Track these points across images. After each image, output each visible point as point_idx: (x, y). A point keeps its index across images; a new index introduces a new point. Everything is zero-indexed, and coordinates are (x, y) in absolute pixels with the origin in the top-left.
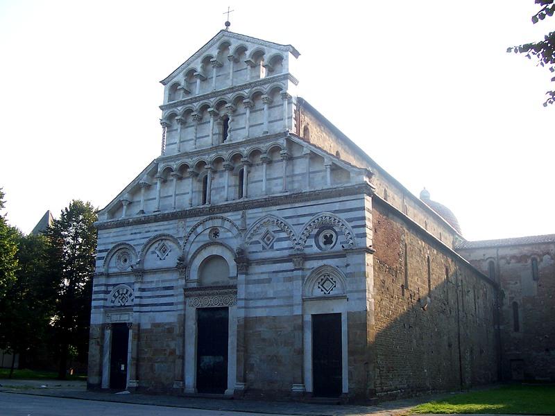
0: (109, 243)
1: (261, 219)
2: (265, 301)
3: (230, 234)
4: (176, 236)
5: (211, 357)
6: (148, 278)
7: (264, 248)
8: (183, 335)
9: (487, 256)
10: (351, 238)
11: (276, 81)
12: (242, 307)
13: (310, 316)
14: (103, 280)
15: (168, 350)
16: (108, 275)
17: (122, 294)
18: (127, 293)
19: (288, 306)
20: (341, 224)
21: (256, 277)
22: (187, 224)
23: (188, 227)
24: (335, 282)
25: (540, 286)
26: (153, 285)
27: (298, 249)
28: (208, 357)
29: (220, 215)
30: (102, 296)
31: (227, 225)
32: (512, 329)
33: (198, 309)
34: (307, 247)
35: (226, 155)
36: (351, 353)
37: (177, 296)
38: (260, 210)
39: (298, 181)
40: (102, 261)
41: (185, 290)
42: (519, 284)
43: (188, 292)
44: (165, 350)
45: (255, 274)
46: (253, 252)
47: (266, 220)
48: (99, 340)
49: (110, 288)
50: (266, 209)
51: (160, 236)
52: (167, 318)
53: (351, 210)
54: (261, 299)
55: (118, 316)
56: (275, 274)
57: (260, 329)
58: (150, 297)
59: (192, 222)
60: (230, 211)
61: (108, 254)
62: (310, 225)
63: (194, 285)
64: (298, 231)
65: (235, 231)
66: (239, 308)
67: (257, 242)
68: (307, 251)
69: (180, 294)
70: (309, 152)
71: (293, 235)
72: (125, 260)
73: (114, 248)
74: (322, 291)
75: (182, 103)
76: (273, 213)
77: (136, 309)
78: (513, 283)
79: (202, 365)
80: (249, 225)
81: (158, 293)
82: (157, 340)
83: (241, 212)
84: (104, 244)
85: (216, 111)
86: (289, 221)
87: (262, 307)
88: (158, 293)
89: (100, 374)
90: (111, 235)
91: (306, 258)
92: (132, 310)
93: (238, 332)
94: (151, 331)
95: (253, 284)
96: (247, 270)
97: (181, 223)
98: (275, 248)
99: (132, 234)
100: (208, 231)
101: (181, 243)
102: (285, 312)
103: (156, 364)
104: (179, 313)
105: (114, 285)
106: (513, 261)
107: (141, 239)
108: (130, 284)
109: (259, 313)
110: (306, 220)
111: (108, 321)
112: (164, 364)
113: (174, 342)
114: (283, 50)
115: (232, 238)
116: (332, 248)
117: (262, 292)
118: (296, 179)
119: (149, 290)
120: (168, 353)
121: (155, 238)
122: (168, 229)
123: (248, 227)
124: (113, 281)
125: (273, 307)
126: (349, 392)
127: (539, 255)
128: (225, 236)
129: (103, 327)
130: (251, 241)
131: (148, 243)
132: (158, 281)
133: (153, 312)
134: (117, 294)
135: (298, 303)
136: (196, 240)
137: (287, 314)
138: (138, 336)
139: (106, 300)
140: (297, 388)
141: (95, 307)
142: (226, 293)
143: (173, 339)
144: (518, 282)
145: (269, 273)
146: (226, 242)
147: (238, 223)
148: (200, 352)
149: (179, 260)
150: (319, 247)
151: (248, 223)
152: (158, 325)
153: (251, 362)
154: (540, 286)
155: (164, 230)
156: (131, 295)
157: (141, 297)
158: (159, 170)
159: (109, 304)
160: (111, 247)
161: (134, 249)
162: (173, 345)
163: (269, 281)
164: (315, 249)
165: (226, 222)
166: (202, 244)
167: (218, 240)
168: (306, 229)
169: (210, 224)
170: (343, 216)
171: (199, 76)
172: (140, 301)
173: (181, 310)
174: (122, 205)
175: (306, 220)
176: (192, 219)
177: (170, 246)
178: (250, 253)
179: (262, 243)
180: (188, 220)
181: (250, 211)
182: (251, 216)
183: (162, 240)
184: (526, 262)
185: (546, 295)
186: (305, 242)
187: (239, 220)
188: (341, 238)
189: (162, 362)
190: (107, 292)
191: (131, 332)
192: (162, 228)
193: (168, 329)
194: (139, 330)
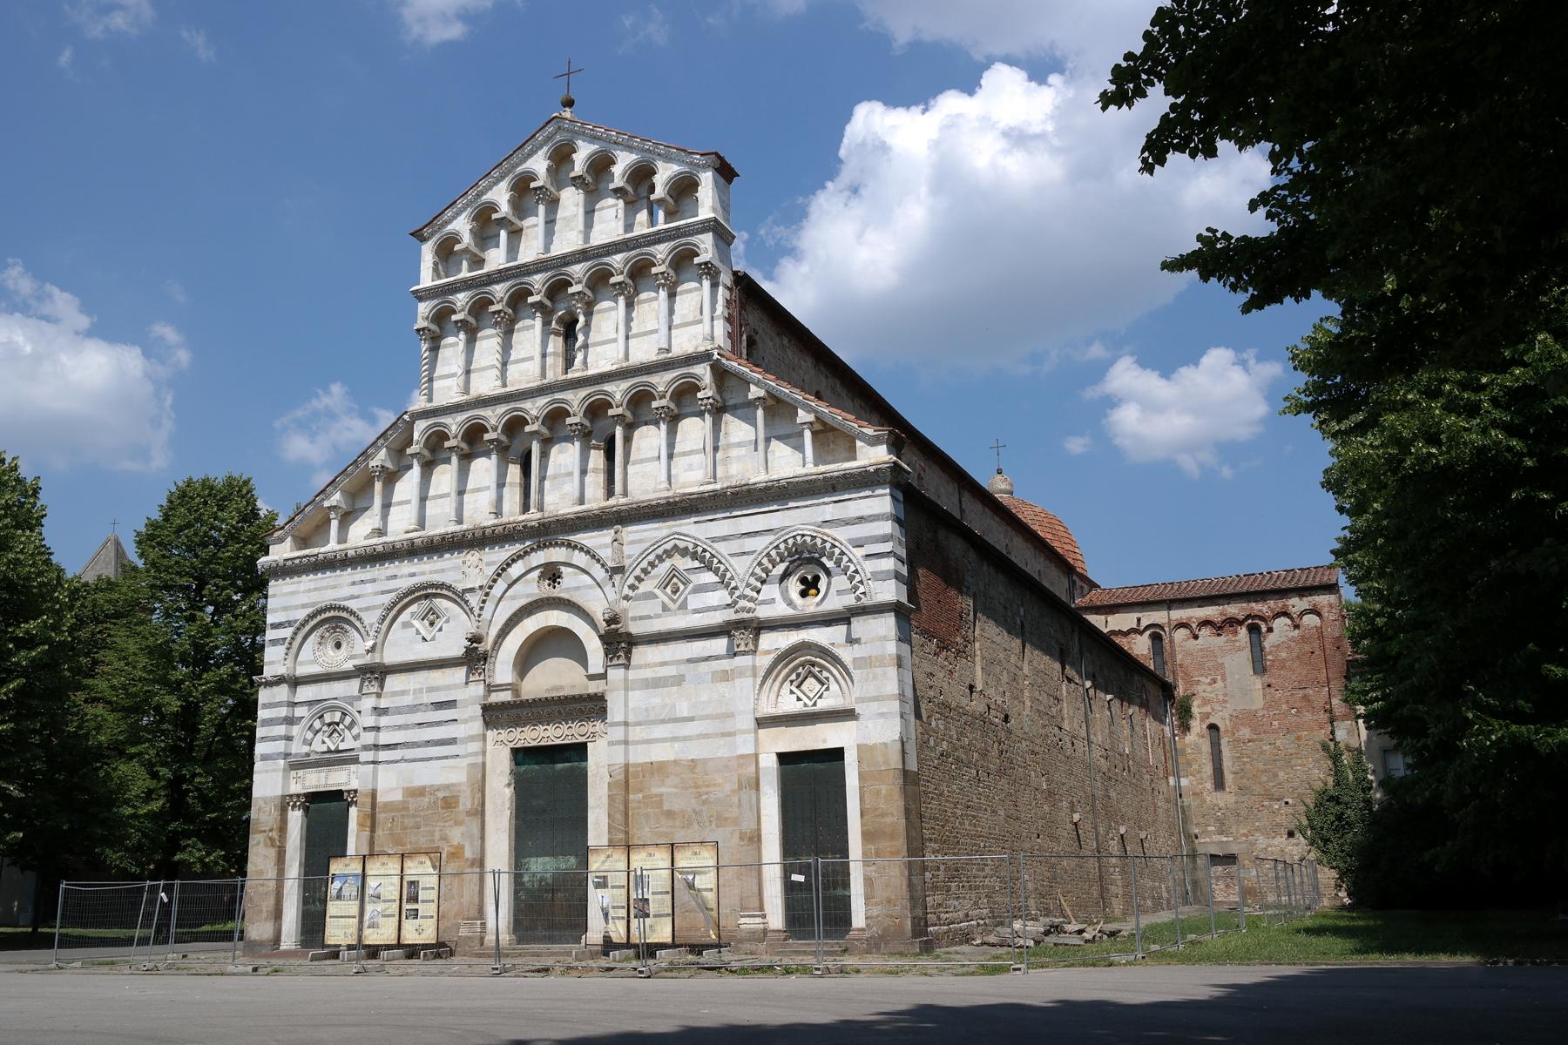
0: (296, 607)
1: (657, 543)
4: (460, 587)
5: (547, 859)
6: (393, 682)
7: (665, 608)
8: (480, 812)
9: (1144, 623)
10: (861, 582)
11: (685, 235)
12: (619, 743)
13: (775, 758)
14: (282, 692)
16: (295, 682)
17: (329, 725)
18: (342, 720)
19: (724, 735)
20: (837, 551)
21: (648, 674)
23: (488, 564)
24: (827, 678)
25: (1269, 686)
26: (408, 700)
27: (743, 609)
28: (540, 860)
30: (281, 730)
31: (579, 558)
32: (1209, 785)
34: (763, 603)
35: (575, 400)
36: (867, 836)
37: (465, 721)
39: (739, 458)
40: (281, 649)
41: (487, 709)
42: (1220, 684)
43: (494, 715)
45: (647, 666)
46: (641, 618)
48: (275, 834)
49: (300, 712)
52: (448, 773)
53: (861, 519)
54: (663, 721)
55: (323, 774)
57: (663, 790)
58: (400, 727)
59: (500, 554)
61: (295, 634)
62: (768, 555)
63: (505, 696)
64: (740, 568)
65: (599, 573)
66: (611, 743)
67: (650, 596)
68: (763, 613)
69: (472, 719)
70: (762, 393)
71: (732, 578)
72: (338, 645)
73: (311, 617)
74: (799, 699)
75: (466, 285)
77: (365, 756)
78: (1208, 680)
79: (526, 879)
80: (629, 557)
81: (419, 717)
84: (285, 609)
85: (548, 303)
86: (722, 548)
87: (664, 740)
88: (419, 717)
89: (278, 914)
90: (302, 587)
91: (759, 627)
92: (355, 761)
93: (611, 798)
94: (401, 807)
95: (641, 689)
96: (629, 659)
97: (473, 557)
99: (354, 583)
100: (536, 573)
101: (474, 600)
102: (719, 750)
104: (472, 760)
105: (310, 703)
106: (1205, 632)
107: (376, 594)
108: (351, 700)
109: (660, 753)
110: (760, 543)
111: (296, 788)
113: (462, 829)
114: (698, 165)
115: (590, 587)
116: (818, 605)
118: (734, 453)
119: (399, 711)
121: (410, 592)
122: (443, 571)
123: (627, 562)
124: (305, 692)
126: (868, 925)
127: (1263, 619)
129: (285, 803)
131: (395, 604)
132: (419, 691)
133: (406, 761)
134: (317, 724)
135: (745, 727)
137: (723, 753)
138: (371, 821)
139: (289, 738)
140: (749, 923)
141: (265, 758)
143: (458, 823)
144: (1219, 678)
145: (678, 662)
146: (577, 598)
147: (606, 554)
148: (521, 851)
149: (470, 640)
150: (790, 603)
151: (627, 550)
152: (420, 792)
154: (1269, 686)
155: (431, 572)
156: (353, 723)
157: (377, 729)
158: (416, 436)
159: (297, 748)
160: (301, 615)
161: (359, 619)
162: (456, 835)
163: (679, 680)
164: (780, 610)
165: (577, 552)
167: (558, 592)
168: (760, 564)
169: (540, 558)
170: (842, 534)
171: (503, 222)
172: (376, 738)
173: (475, 754)
174: (329, 521)
175: (760, 543)
177: (446, 609)
178: (634, 619)
181: (630, 528)
183: (427, 596)
184: (1235, 633)
185: (1284, 706)
186: (758, 592)
187: (606, 546)
188: (840, 582)
190: (290, 721)
191: (353, 811)
194: (374, 805)
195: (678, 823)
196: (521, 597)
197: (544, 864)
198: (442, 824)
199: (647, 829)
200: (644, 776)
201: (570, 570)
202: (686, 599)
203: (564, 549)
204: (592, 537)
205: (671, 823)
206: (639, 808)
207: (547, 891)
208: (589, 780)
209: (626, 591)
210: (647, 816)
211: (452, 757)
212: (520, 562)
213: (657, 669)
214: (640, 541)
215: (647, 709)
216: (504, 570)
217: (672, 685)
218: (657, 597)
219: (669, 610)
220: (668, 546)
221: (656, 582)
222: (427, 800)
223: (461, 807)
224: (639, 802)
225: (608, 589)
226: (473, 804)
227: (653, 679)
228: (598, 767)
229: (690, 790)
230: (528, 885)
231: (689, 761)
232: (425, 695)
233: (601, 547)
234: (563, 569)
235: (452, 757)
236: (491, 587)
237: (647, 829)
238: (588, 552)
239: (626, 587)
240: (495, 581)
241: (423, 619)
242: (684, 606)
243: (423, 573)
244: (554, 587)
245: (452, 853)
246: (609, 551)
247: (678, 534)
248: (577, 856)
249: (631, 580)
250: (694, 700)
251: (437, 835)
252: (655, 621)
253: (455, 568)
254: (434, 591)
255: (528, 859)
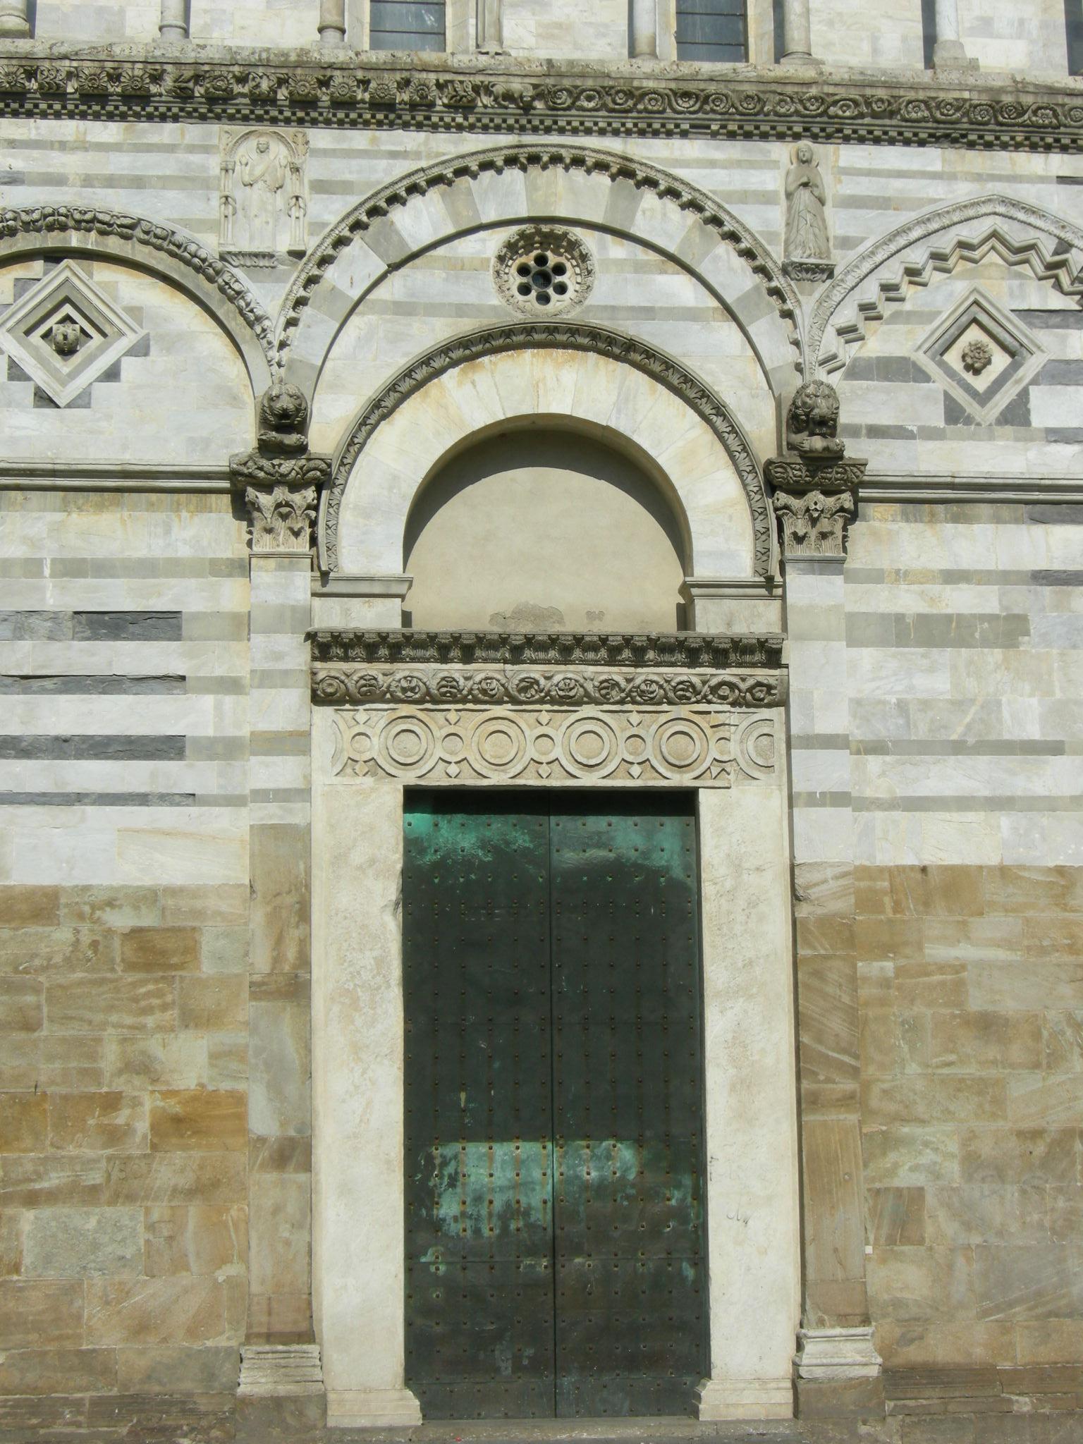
2: (983, 761)
3: (682, 289)
4: (209, 245)
5: (528, 1149)
7: (954, 414)
15: (149, 1103)
21: (908, 601)
22: (314, 169)
23: (321, 187)
28: (503, 1151)
29: (614, 145)
33: (416, 798)
38: (932, 158)
44: (112, 1102)
45: (901, 576)
46: (876, 432)
47: (985, 226)
50: (977, 160)
51: (55, 222)
54: (958, 748)
56: (1047, 590)
57: (964, 952)
60: (699, 129)
69: (266, 679)
76: (1027, 193)
79: (448, 1208)
80: (846, 243)
82: (29, 1026)
83: (781, 151)
87: (964, 803)
95: (882, 642)
98: (1039, 420)
103: (28, 1219)
112: (122, 1213)
115: (691, 315)
117: (959, 705)
120: (143, 1127)
122: (138, 183)
123: (840, 259)
125: (1049, 804)
128: (633, 296)
130: (849, 353)
136: (381, 293)
142: (684, 694)
143: (192, 1019)
145: (1005, 578)
151: (838, 222)
153: (905, 1179)
155: (88, 181)
165: (649, 198)
166: (437, 332)
176: (359, 139)
178: (854, 431)
179: (941, 382)
180: (321, 138)
182: (850, 187)
183: (53, 256)
187: (766, 198)
189: (91, 1195)
192: (71, 163)
193: (136, 934)
195: (1016, 1052)
196: (433, 310)
197: (518, 1163)
198: (129, 1020)
199: (913, 1068)
200: (897, 908)
201: (619, 250)
202: (1024, 395)
203: (602, 179)
204: (712, 164)
205: (993, 1052)
206: (883, 1002)
207: (532, 1251)
208: (707, 908)
209: (831, 343)
210: (912, 1028)
211: (165, 799)
212: (434, 193)
213: (935, 589)
214: (883, 203)
215: (902, 706)
216: (374, 212)
217: (986, 643)
218: (927, 378)
219: (969, 420)
220: (973, 232)
221: (922, 333)
222: (62, 935)
223: (207, 968)
224: (885, 983)
225: (768, 330)
226: (277, 960)
227: (923, 619)
228: (737, 866)
229: (1055, 957)
230: (454, 1228)
231: (1050, 870)
232: (49, 583)
233: (745, 197)
234: (589, 240)
235: (165, 799)
236: (325, 261)
237: (913, 1068)
238: (694, 205)
239: (830, 331)
240: (341, 242)
241: (28, 332)
242: (1017, 415)
243: (57, 180)
244: (544, 299)
245: (177, 1120)
246: (776, 216)
247: (1004, 201)
248: (639, 1142)
249: (848, 314)
250: (1058, 695)
251: (110, 1056)
252: (922, 446)
253: (190, 181)
254: (91, 241)
255: (454, 1148)
